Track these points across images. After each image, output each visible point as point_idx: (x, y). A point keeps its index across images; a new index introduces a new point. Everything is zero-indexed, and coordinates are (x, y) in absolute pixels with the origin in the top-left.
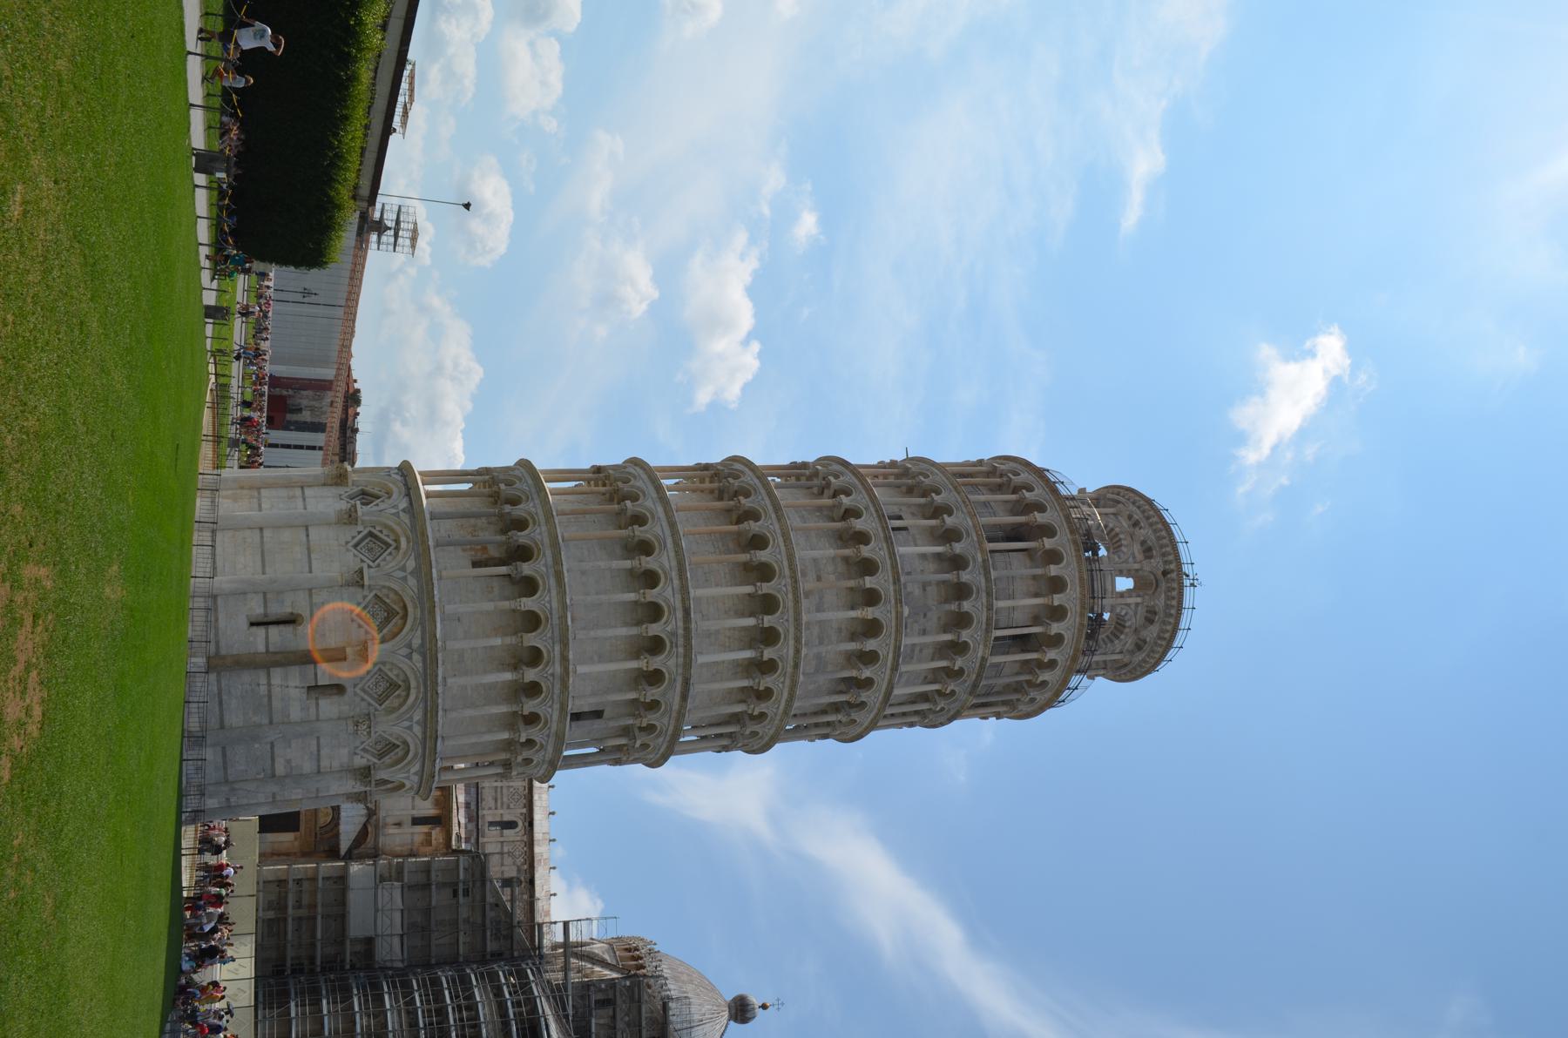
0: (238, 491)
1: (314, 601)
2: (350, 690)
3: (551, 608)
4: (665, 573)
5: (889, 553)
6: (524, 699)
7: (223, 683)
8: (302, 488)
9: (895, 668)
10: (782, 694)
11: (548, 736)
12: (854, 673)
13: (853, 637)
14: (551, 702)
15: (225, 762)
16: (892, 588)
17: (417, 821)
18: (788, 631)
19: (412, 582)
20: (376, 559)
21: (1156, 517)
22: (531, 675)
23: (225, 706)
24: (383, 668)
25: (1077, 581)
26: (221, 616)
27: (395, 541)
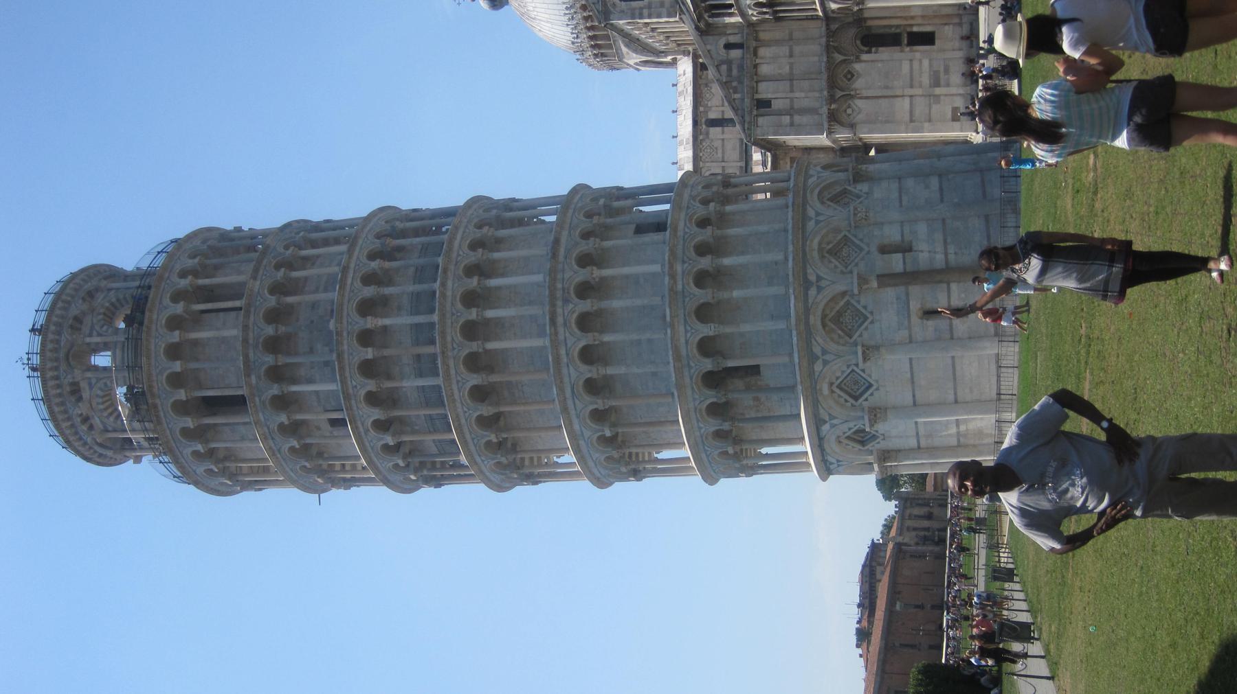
0: (977, 442)
2: (874, 249)
3: (685, 326)
6: (711, 240)
8: (919, 448)
9: (345, 270)
10: (460, 245)
11: (688, 208)
12: (387, 265)
14: (686, 236)
16: (346, 347)
18: (452, 304)
19: (817, 350)
20: (851, 372)
22: (705, 262)
24: (844, 269)
25: (153, 355)
27: (833, 392)
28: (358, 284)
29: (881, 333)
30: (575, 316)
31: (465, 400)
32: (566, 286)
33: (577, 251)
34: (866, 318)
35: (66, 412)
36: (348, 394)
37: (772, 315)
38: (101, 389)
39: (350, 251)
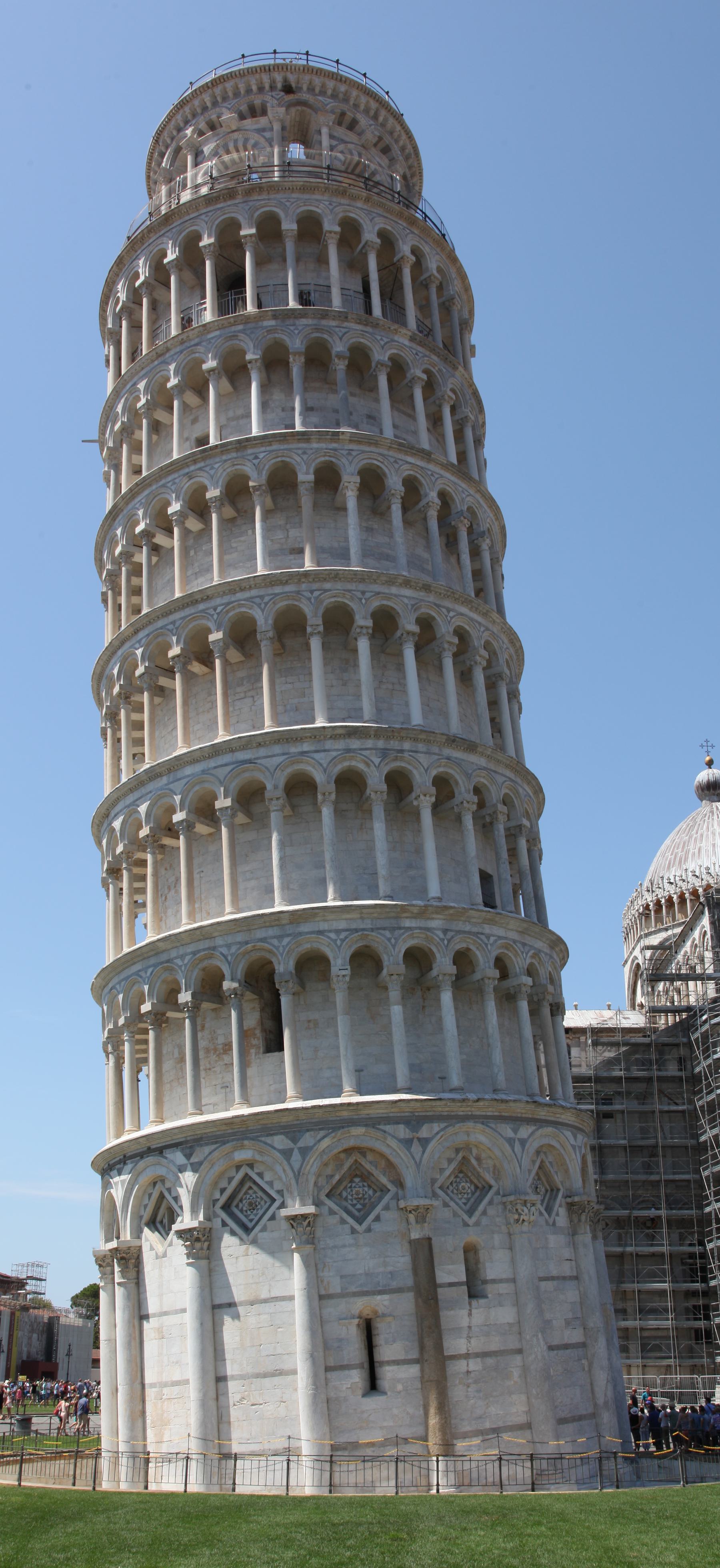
1: (339, 1290)
4: (293, 763)
5: (262, 444)
6: (477, 976)
7: (466, 1427)
9: (426, 455)
11: (524, 944)
14: (483, 937)
16: (315, 445)
18: (379, 593)
19: (307, 1139)
21: (204, 96)
23: (500, 1424)
25: (306, 196)
27: (238, 1168)
29: (335, 1247)
30: (361, 766)
31: (234, 608)
32: (406, 755)
33: (457, 777)
34: (360, 1221)
35: (225, 99)
36: (245, 447)
37: (362, 1070)
39: (448, 466)
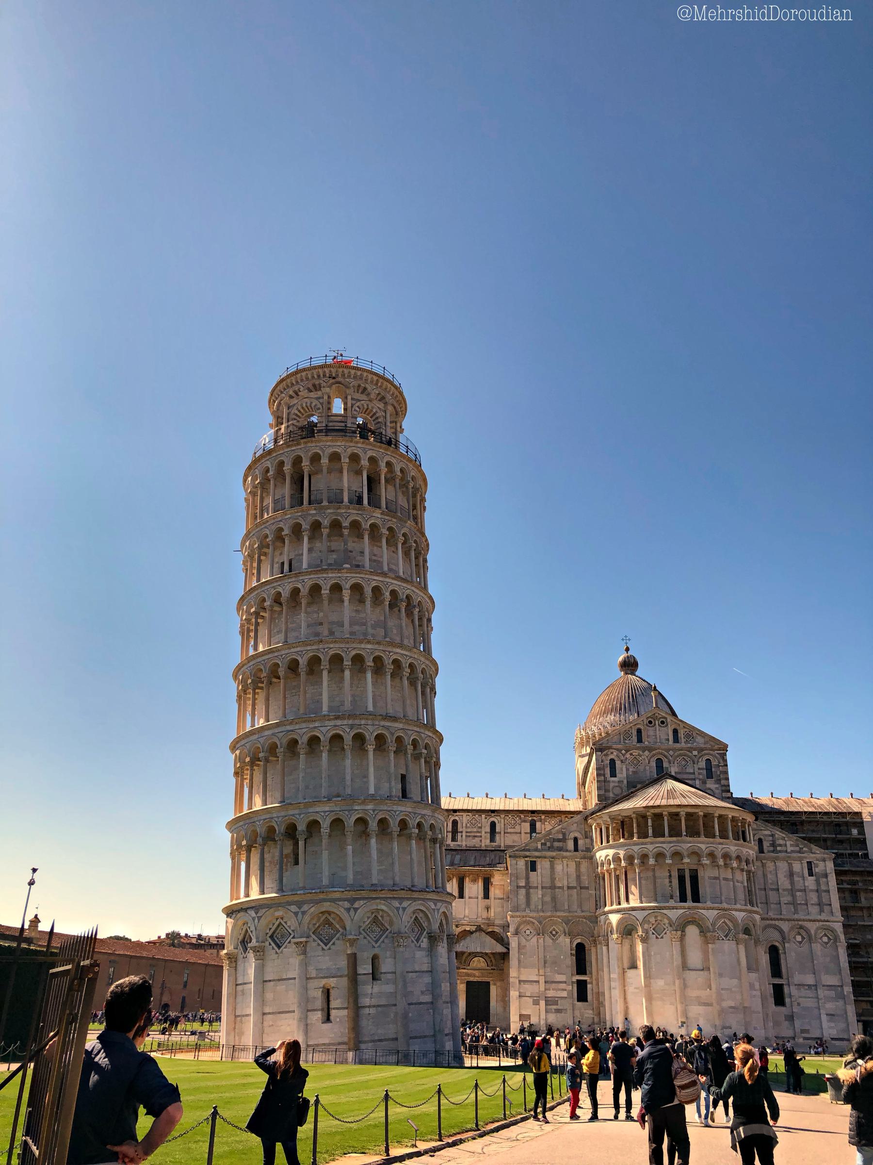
0: (236, 1030)
2: (376, 951)
4: (311, 732)
6: (389, 830)
7: (366, 1039)
8: (237, 985)
10: (397, 653)
11: (415, 813)
13: (362, 601)
15: (420, 1037)
17: (486, 896)
19: (305, 908)
21: (292, 378)
22: (373, 825)
26: (321, 1041)
27: (277, 919)
28: (374, 584)
30: (341, 733)
31: (289, 656)
33: (387, 734)
34: (326, 945)
38: (316, 405)
